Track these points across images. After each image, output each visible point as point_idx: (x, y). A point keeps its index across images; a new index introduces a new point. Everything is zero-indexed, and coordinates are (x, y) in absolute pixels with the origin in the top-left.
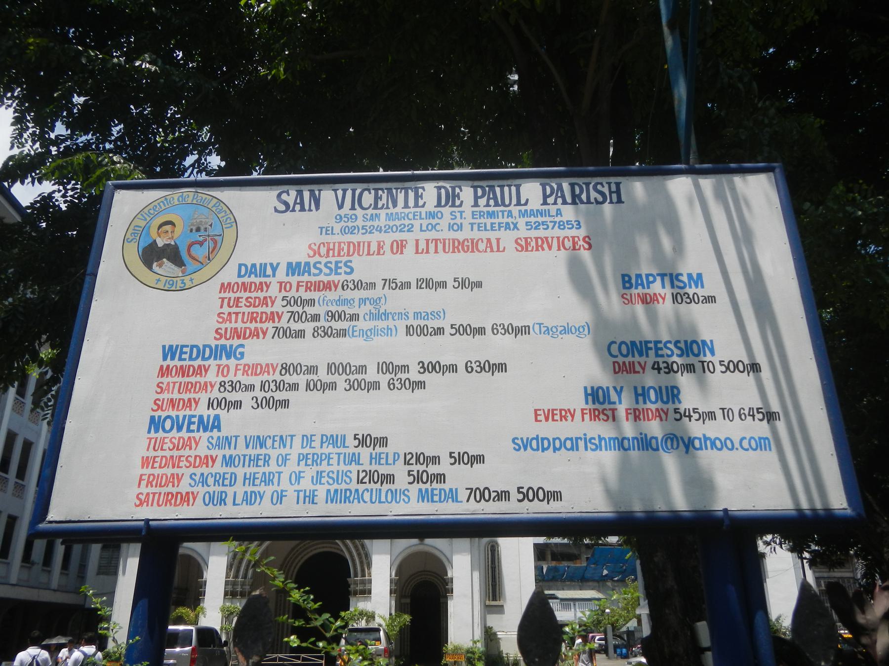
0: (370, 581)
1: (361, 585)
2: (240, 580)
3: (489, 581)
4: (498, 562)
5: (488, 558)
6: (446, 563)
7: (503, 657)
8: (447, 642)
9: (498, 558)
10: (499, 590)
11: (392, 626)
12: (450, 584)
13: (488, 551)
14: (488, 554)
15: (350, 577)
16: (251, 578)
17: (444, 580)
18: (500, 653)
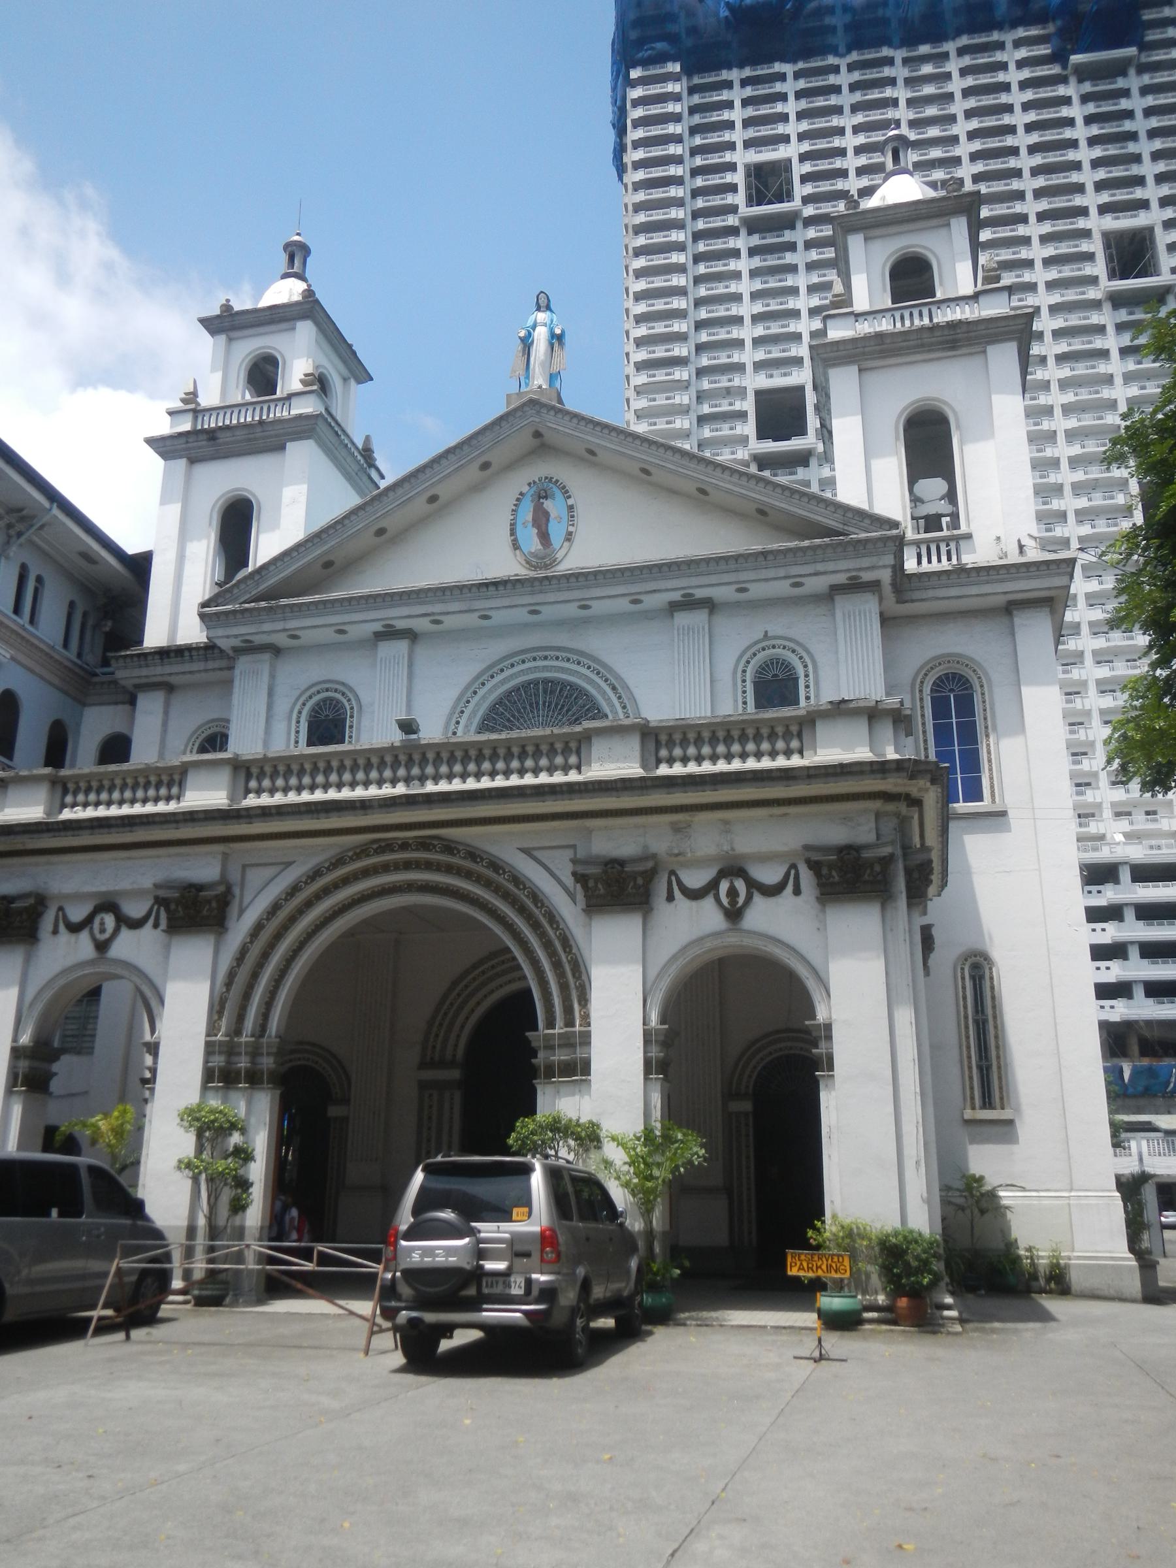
0: (586, 1040)
1: (565, 1051)
2: (243, 1039)
3: (969, 1057)
4: (994, 1007)
5: (965, 998)
6: (811, 984)
7: (1019, 1257)
8: (819, 1212)
9: (993, 998)
10: (1000, 1078)
11: (645, 1163)
12: (823, 1044)
13: (963, 978)
14: (964, 988)
15: (536, 1029)
16: (276, 1037)
17: (807, 1031)
18: (1011, 1245)
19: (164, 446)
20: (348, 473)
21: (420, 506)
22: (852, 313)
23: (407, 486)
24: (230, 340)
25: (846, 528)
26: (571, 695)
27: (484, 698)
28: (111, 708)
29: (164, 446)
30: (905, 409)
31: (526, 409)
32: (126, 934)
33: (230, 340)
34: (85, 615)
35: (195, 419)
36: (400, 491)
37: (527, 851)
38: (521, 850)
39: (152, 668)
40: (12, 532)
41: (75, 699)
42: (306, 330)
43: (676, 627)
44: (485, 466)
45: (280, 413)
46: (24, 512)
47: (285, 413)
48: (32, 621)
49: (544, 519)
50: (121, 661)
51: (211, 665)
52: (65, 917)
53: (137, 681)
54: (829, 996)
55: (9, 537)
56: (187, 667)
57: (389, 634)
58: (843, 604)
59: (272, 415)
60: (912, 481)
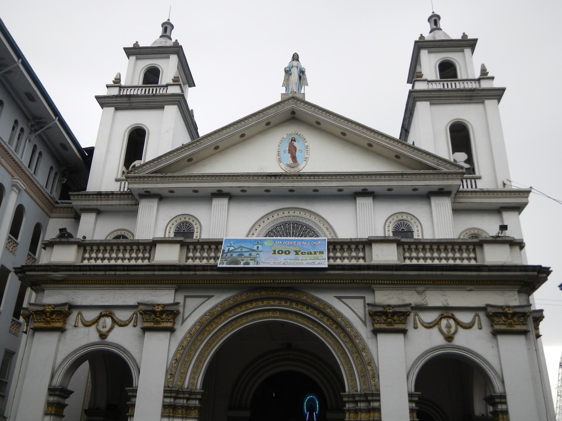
19: (103, 101)
20: (188, 123)
21: (237, 138)
22: (426, 80)
23: (232, 128)
24: (137, 59)
25: (438, 167)
26: (306, 231)
27: (263, 228)
28: (65, 219)
29: (103, 101)
30: (450, 121)
31: (290, 101)
32: (117, 328)
33: (137, 59)
34: (56, 174)
35: (120, 90)
36: (228, 130)
37: (339, 298)
38: (334, 297)
39: (92, 202)
40: (33, 129)
41: (47, 214)
42: (174, 59)
43: (357, 204)
44: (268, 124)
45: (162, 91)
46: (42, 120)
47: (164, 92)
48: (34, 174)
49: (294, 150)
50: (76, 197)
51: (122, 202)
52: (82, 316)
53: (83, 207)
54: (503, 382)
55: (31, 131)
56: (110, 202)
57: (220, 194)
58: (435, 201)
59: (158, 92)
60: (453, 153)
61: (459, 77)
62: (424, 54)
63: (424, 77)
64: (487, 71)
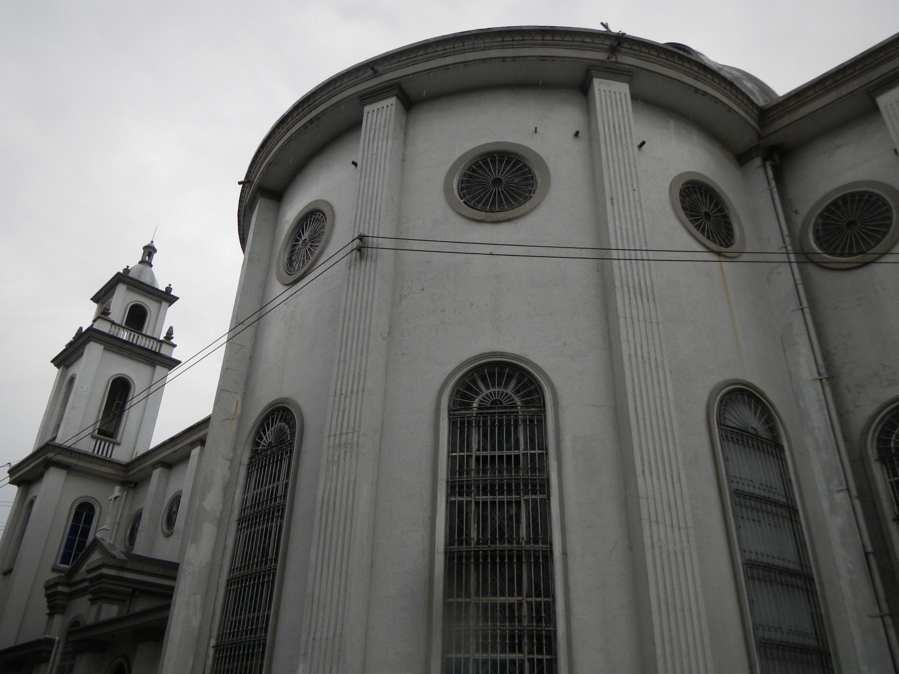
61: (144, 332)
62: (121, 289)
63: (111, 317)
64: (172, 336)
